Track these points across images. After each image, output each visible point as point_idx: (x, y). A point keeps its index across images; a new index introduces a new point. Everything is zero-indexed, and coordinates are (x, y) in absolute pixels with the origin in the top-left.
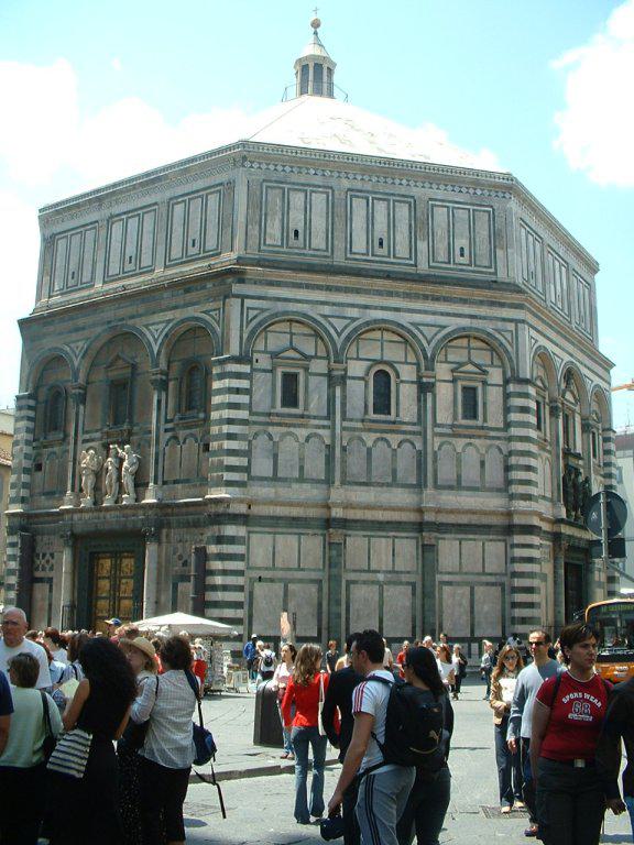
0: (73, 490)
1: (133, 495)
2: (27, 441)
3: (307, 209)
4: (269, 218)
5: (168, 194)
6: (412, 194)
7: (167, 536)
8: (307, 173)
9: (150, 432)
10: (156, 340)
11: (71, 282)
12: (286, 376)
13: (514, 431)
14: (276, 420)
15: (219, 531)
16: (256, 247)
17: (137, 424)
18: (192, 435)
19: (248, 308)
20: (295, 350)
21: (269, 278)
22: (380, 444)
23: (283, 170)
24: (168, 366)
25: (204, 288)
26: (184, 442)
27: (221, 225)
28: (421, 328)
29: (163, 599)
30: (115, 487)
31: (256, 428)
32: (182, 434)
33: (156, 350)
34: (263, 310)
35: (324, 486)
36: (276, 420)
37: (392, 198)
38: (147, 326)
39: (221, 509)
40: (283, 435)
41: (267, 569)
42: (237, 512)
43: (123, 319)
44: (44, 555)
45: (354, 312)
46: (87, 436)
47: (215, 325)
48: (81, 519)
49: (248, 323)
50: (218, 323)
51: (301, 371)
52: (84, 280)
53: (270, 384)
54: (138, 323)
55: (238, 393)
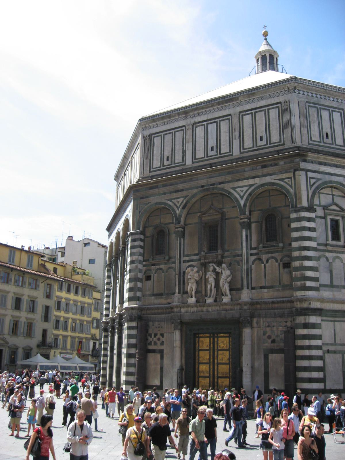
0: (179, 293)
1: (229, 296)
2: (140, 260)
3: (331, 121)
4: (312, 124)
5: (239, 109)
7: (257, 323)
8: (329, 100)
9: (241, 255)
10: (242, 198)
11: (166, 163)
12: (332, 220)
14: (330, 248)
15: (305, 320)
16: (307, 141)
17: (228, 251)
18: (273, 258)
19: (310, 178)
20: (337, 205)
21: (320, 160)
23: (316, 97)
24: (250, 214)
25: (276, 165)
26: (267, 262)
27: (282, 127)
29: (256, 364)
31: (321, 253)
32: (264, 257)
33: (242, 203)
34: (318, 180)
36: (330, 248)
38: (234, 189)
39: (305, 305)
40: (335, 258)
41: (332, 344)
42: (316, 307)
43: (214, 184)
44: (155, 335)
46: (187, 258)
48: (187, 312)
49: (310, 190)
50: (291, 186)
51: (340, 219)
52: (176, 162)
53: (324, 225)
54: (226, 186)
55: (310, 231)
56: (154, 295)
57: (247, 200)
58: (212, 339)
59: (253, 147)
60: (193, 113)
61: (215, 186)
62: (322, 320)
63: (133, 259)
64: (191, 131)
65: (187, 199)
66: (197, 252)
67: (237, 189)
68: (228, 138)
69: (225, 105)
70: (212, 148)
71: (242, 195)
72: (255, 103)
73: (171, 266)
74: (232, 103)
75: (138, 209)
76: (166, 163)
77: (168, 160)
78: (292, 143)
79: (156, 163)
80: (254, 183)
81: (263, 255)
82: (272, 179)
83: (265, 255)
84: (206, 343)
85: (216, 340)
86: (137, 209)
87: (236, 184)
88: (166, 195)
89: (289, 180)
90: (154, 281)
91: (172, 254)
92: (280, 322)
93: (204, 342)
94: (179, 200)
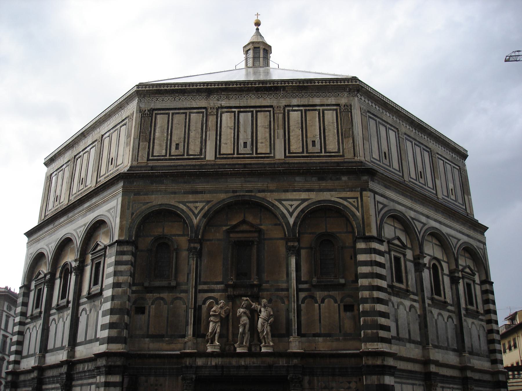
5: (284, 102)
6: (430, 147)
7: (310, 383)
10: (291, 214)
13: (487, 317)
17: (267, 282)
19: (378, 202)
22: (440, 317)
26: (323, 301)
28: (451, 238)
30: (247, 337)
32: (319, 295)
35: (421, 347)
37: (422, 146)
38: (280, 201)
43: (251, 191)
45: (423, 219)
46: (205, 287)
47: (354, 209)
50: (357, 209)
54: (271, 197)
56: (148, 336)
57: (297, 217)
59: (303, 152)
61: (253, 194)
62: (395, 382)
63: (118, 280)
64: (215, 116)
65: (210, 205)
66: (221, 280)
67: (283, 202)
68: (268, 135)
70: (245, 144)
71: (291, 210)
72: (306, 99)
73: (178, 295)
75: (131, 209)
76: (173, 151)
77: (177, 148)
78: (354, 156)
79: (159, 150)
80: (308, 198)
81: (318, 293)
82: (332, 196)
83: (320, 292)
86: (128, 209)
87: (283, 196)
88: (177, 195)
89: (354, 200)
90: (149, 316)
91: (182, 278)
92: (341, 383)
94: (198, 204)
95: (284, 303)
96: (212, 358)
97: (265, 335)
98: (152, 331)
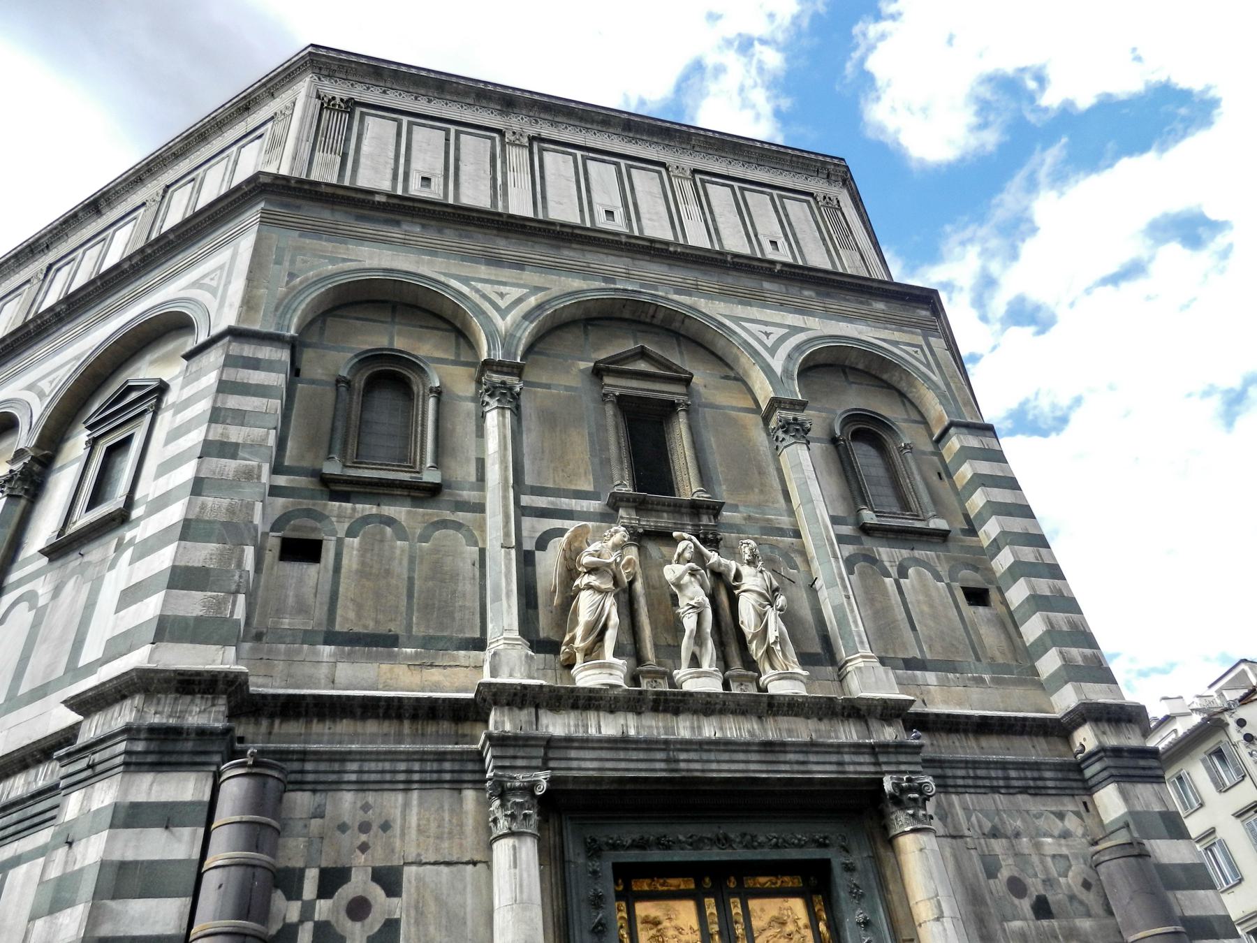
10: (773, 351)
18: (918, 562)
26: (903, 573)
46: (542, 502)
50: (928, 366)
56: (331, 638)
58: (711, 907)
60: (531, 114)
69: (645, 138)
71: (769, 343)
74: (667, 142)
75: (287, 264)
84: (679, 929)
85: (736, 910)
87: (740, 310)
90: (337, 569)
93: (666, 924)
95: (795, 567)
96: (602, 714)
97: (775, 643)
98: (346, 620)
